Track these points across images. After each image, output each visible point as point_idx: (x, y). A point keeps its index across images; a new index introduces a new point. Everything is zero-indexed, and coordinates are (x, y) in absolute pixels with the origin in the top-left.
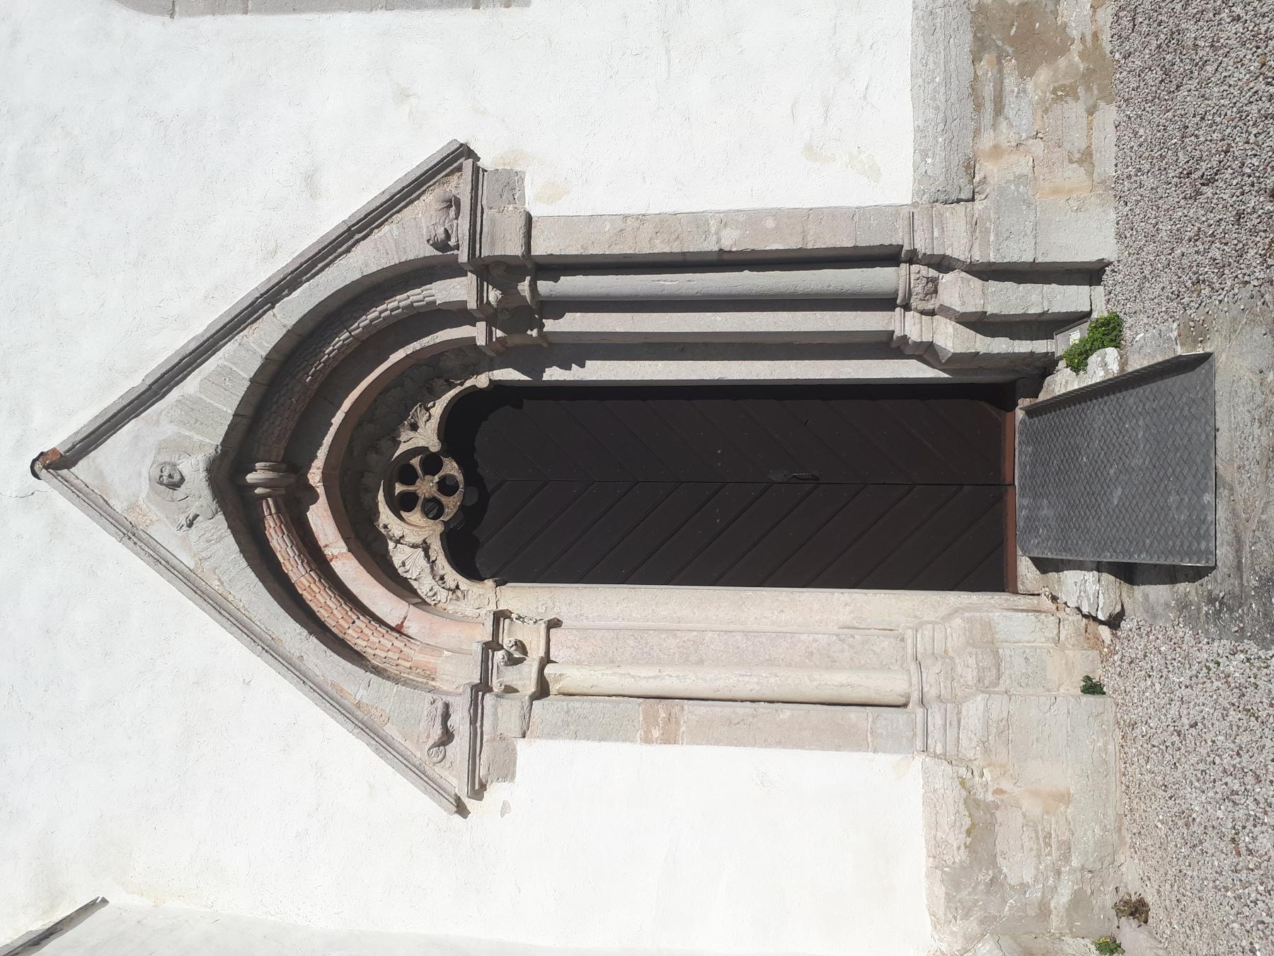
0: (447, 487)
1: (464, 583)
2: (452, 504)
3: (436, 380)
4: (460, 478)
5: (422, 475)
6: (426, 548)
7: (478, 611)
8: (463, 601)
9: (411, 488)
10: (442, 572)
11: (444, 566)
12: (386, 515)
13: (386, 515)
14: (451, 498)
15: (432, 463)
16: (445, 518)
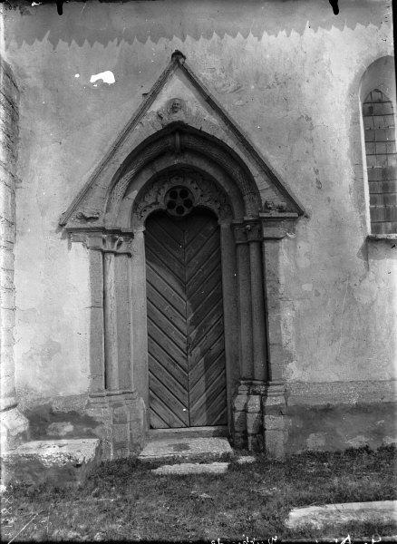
1: (144, 218)
2: (173, 212)
6: (156, 203)
11: (150, 211)
12: (167, 187)
13: (167, 187)
15: (188, 203)
16: (169, 211)
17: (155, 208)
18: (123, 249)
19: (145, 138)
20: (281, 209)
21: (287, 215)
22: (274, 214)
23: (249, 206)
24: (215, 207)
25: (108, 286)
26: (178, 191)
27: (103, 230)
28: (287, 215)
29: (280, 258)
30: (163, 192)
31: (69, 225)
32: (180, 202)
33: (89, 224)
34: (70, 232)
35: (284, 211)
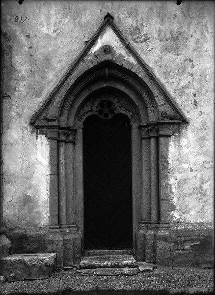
1: (83, 121)
2: (102, 117)
4: (109, 118)
6: (91, 111)
11: (86, 116)
15: (112, 111)
16: (100, 116)
17: (90, 114)
18: (71, 139)
19: (86, 70)
20: (171, 118)
21: (175, 121)
22: (167, 120)
23: (150, 114)
24: (129, 114)
25: (61, 162)
26: (105, 103)
27: (59, 127)
28: (175, 121)
29: (170, 148)
30: (96, 104)
31: (37, 123)
32: (106, 110)
33: (50, 124)
34: (37, 128)
35: (173, 119)
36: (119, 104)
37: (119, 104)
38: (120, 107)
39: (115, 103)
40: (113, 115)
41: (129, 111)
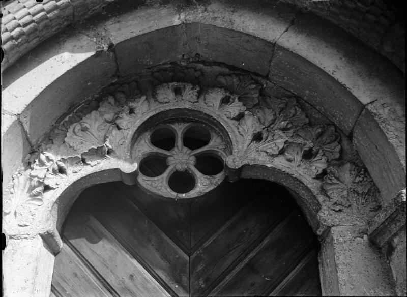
0: (182, 181)
1: (51, 197)
2: (159, 186)
3: (324, 159)
4: (193, 194)
5: (193, 154)
7: (13, 213)
8: (28, 195)
9: (179, 142)
10: (70, 169)
12: (144, 110)
14: (165, 184)
15: (211, 164)
16: (143, 180)
30: (130, 124)
36: (250, 125)
37: (250, 125)
38: (258, 138)
39: (230, 126)
40: (219, 178)
41: (308, 155)
